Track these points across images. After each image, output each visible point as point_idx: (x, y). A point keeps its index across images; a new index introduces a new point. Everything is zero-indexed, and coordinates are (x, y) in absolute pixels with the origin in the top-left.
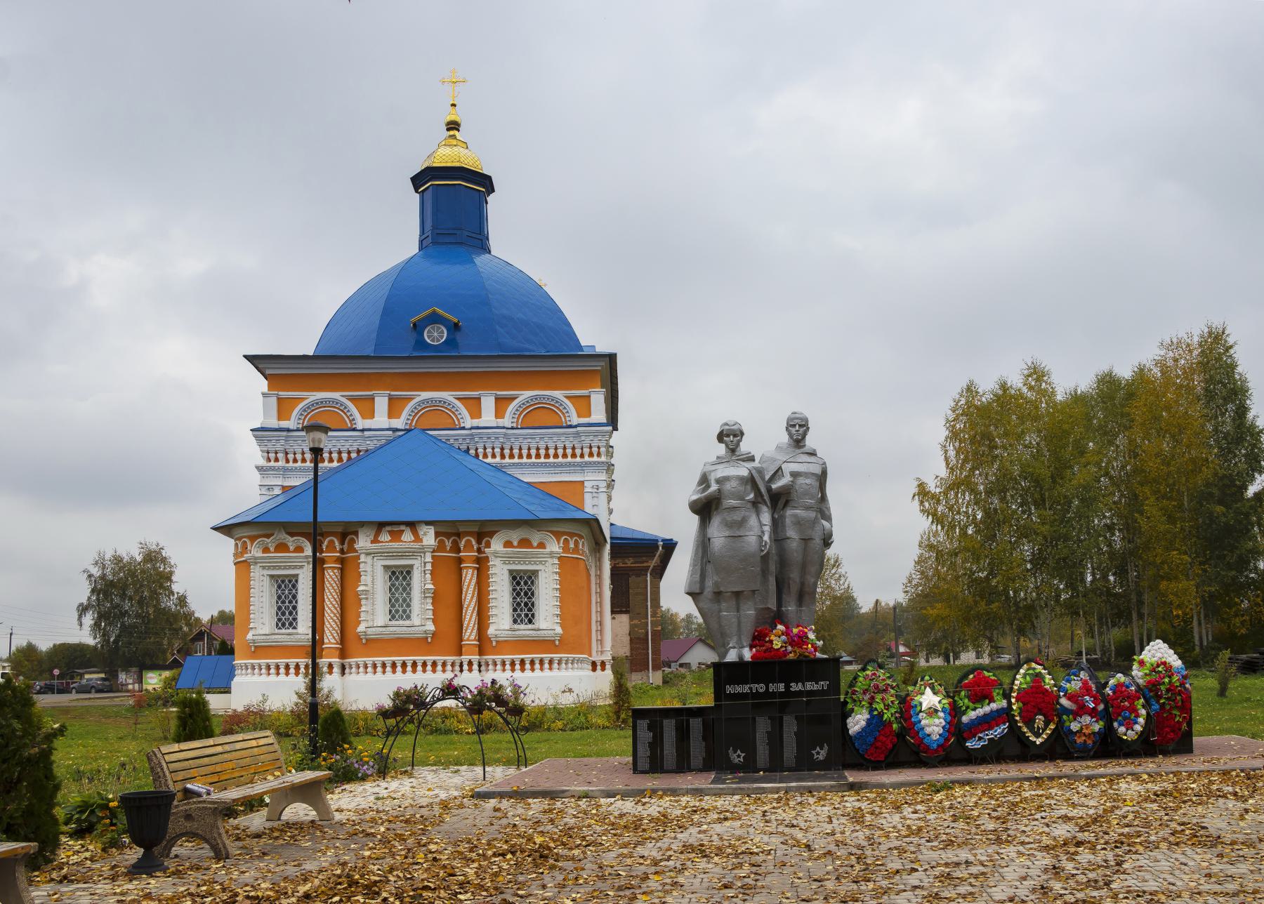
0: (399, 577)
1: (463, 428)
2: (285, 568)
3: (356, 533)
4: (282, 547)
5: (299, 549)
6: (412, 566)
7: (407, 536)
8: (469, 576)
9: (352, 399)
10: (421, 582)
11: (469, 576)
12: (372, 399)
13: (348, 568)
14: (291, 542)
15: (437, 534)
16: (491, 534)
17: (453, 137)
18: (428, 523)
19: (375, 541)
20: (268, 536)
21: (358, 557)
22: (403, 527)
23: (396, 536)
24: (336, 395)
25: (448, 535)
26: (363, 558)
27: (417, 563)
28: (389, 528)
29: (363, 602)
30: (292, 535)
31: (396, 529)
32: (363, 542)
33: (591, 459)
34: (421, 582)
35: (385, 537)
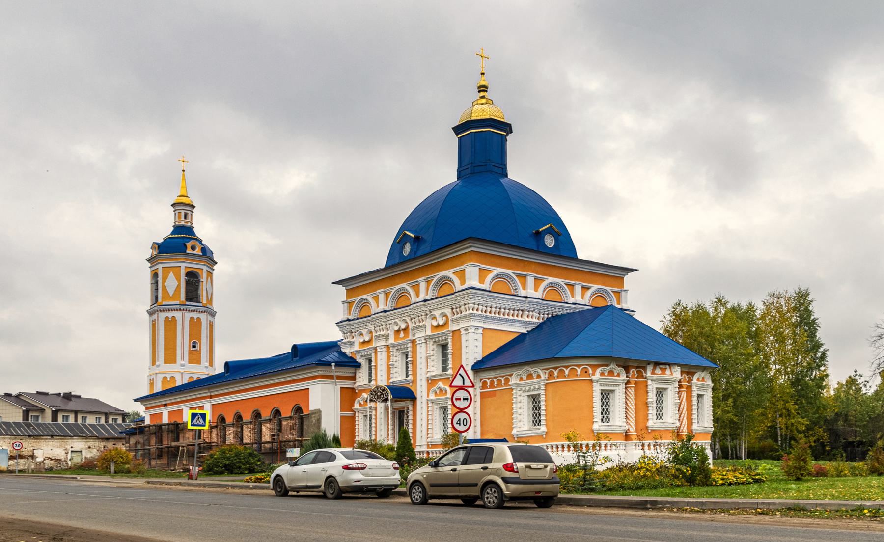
0: (660, 392)
2: (611, 386)
3: (645, 369)
4: (611, 373)
5: (618, 375)
6: (665, 389)
7: (668, 372)
8: (684, 395)
9: (518, 275)
10: (671, 397)
12: (525, 277)
13: (641, 388)
14: (618, 370)
15: (682, 373)
16: (693, 374)
17: (483, 97)
18: (679, 365)
19: (653, 373)
20: (607, 365)
21: (647, 382)
23: (663, 371)
24: (509, 272)
25: (688, 373)
26: (650, 383)
27: (670, 387)
29: (650, 408)
30: (619, 366)
32: (649, 374)
33: (527, 319)
34: (671, 397)
35: (658, 371)
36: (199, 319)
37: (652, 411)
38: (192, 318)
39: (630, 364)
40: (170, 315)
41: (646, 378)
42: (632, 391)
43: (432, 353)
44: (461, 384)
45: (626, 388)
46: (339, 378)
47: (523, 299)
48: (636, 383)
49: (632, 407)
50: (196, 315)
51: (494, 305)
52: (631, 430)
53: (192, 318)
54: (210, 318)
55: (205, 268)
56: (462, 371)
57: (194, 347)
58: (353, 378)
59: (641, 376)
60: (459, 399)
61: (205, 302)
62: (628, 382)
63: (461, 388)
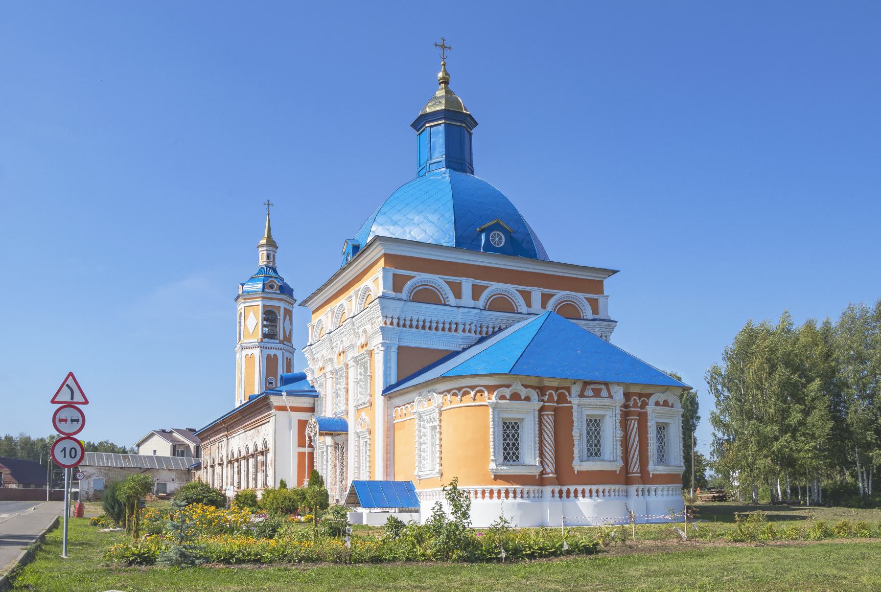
1: (521, 313)
4: (515, 397)
6: (603, 416)
8: (634, 425)
11: (634, 425)
16: (649, 396)
18: (618, 384)
20: (508, 386)
22: (603, 386)
28: (593, 386)
31: (598, 387)
36: (275, 356)
37: (579, 447)
38: (269, 355)
39: (547, 384)
40: (249, 352)
41: (570, 402)
42: (549, 420)
43: (359, 377)
44: (68, 399)
45: (540, 416)
46: (294, 409)
47: (455, 309)
48: (555, 409)
49: (549, 439)
50: (272, 353)
51: (415, 318)
52: (548, 470)
53: (269, 355)
54: (287, 354)
55: (282, 305)
56: (70, 382)
57: (271, 383)
58: (312, 410)
59: (562, 399)
60: (66, 420)
61: (281, 338)
62: (541, 410)
63: (69, 405)
